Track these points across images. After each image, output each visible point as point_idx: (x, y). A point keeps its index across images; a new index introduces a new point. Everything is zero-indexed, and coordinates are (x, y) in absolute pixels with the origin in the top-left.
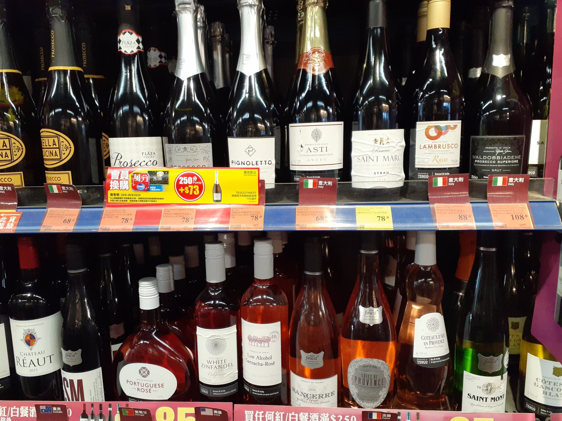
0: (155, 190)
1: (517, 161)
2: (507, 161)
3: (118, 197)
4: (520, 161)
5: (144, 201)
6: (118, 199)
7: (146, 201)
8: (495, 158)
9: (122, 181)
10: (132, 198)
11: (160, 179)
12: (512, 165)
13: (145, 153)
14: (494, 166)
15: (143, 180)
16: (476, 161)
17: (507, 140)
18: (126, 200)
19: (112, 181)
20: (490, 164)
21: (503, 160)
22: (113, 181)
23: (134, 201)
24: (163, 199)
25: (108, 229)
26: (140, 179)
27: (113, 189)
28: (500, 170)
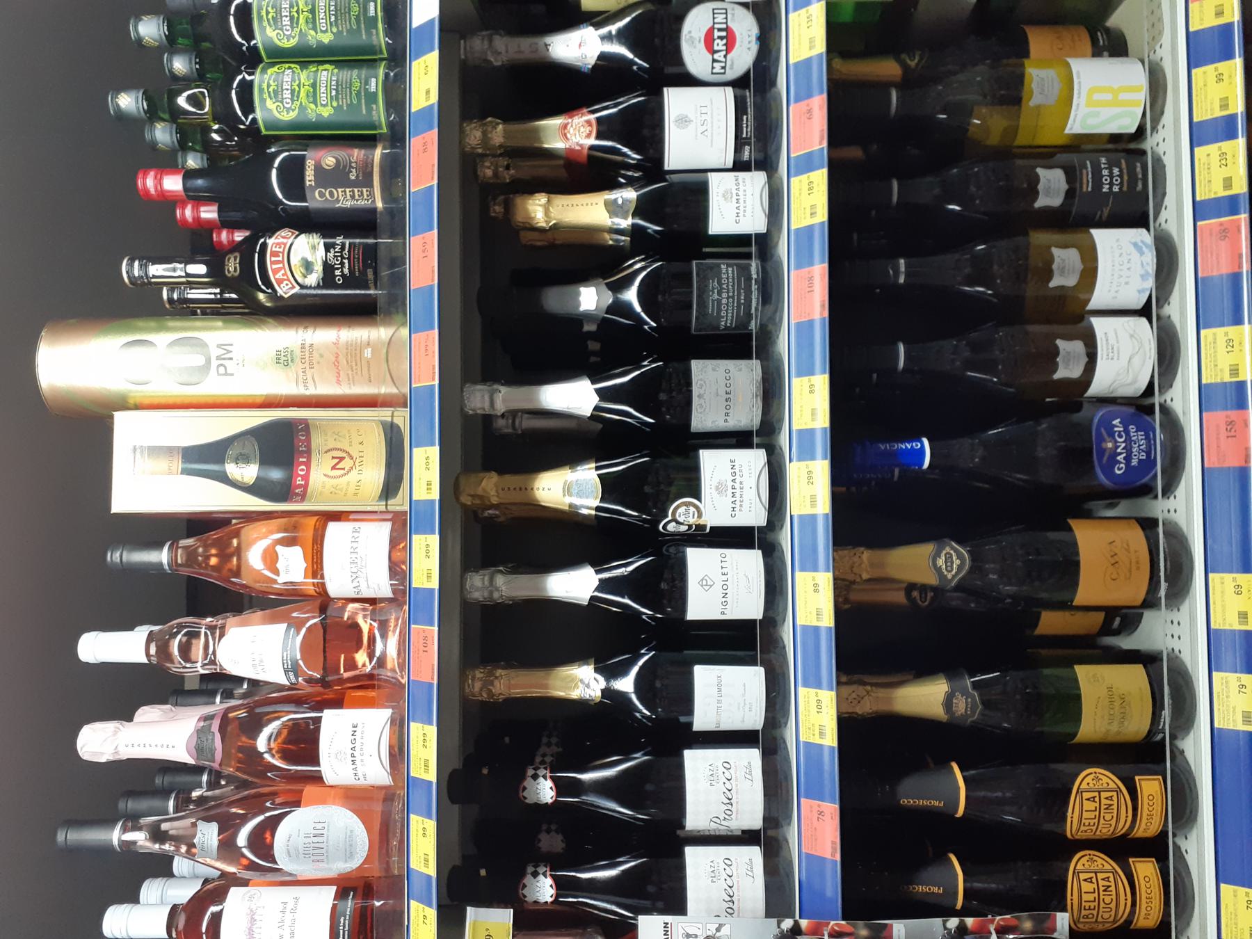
4: (728, 266)
16: (728, 325)
21: (728, 289)
25: (833, 843)
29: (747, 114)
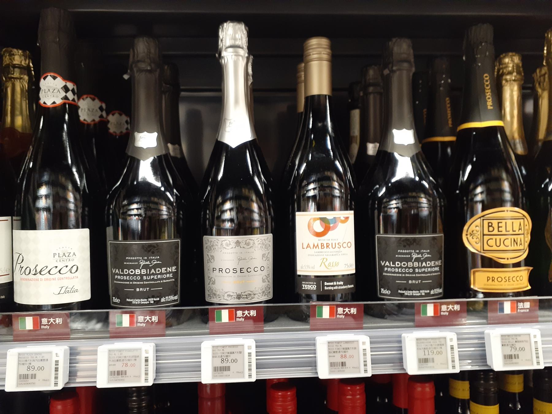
1: (438, 268)
2: (155, 276)
4: (175, 274)
8: (139, 271)
12: (164, 281)
13: (57, 255)
14: (138, 283)
17: (154, 247)
20: (133, 281)
21: (150, 275)
28: (148, 289)
29: (344, 285)
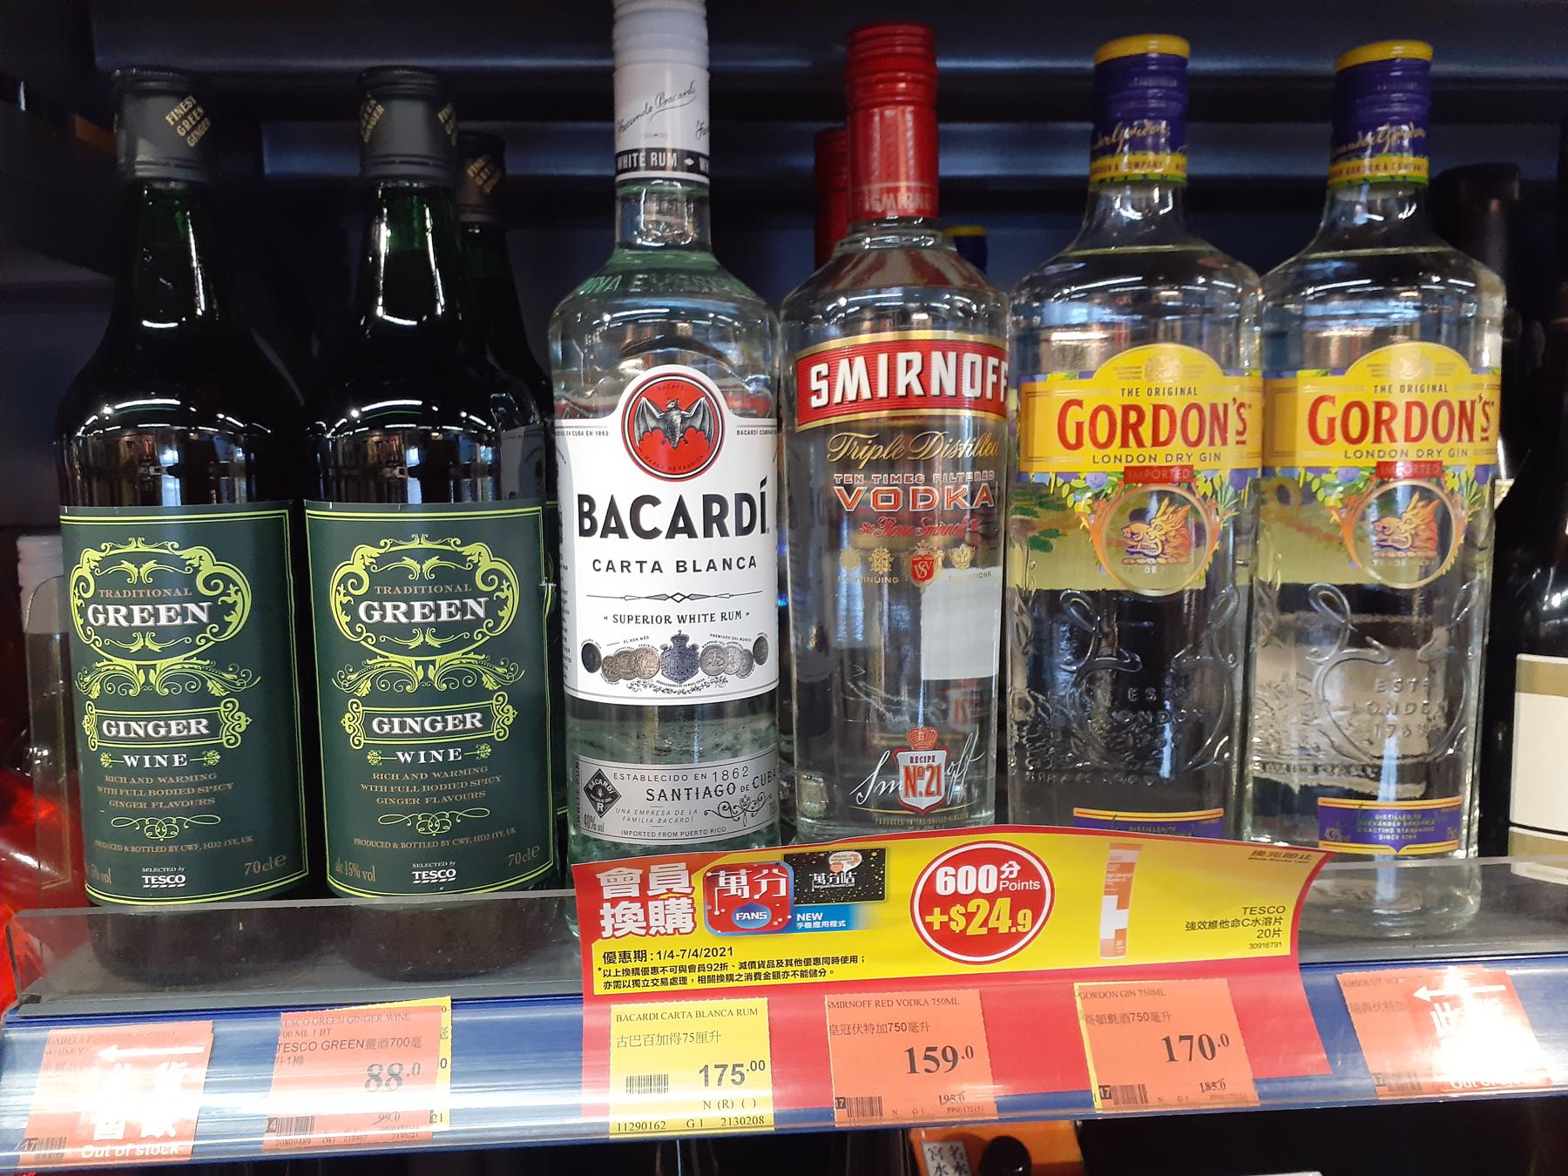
0: (817, 925)
3: (640, 965)
5: (767, 976)
6: (641, 977)
7: (776, 975)
9: (660, 903)
10: (710, 967)
11: (847, 881)
15: (764, 888)
18: (678, 975)
19: (607, 906)
22: (613, 906)
23: (721, 978)
24: (854, 959)
26: (747, 889)
27: (618, 934)
